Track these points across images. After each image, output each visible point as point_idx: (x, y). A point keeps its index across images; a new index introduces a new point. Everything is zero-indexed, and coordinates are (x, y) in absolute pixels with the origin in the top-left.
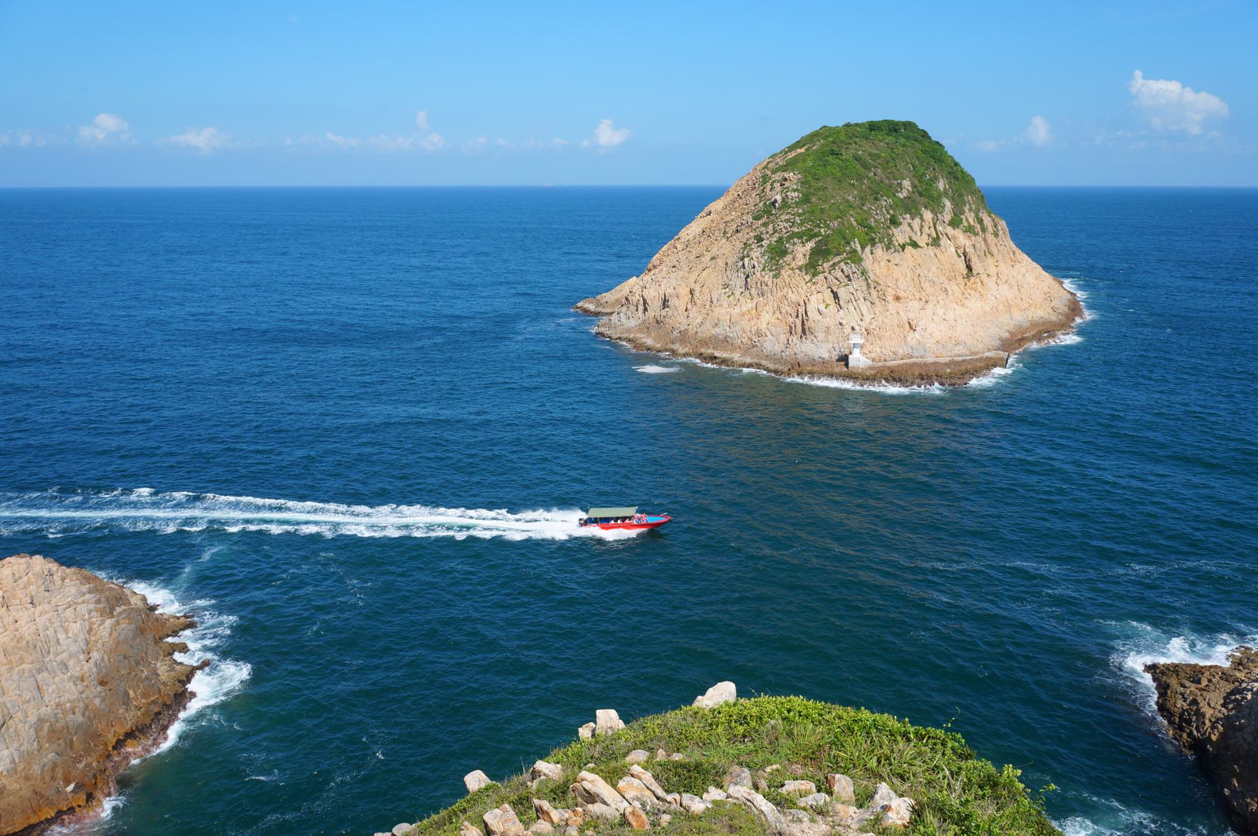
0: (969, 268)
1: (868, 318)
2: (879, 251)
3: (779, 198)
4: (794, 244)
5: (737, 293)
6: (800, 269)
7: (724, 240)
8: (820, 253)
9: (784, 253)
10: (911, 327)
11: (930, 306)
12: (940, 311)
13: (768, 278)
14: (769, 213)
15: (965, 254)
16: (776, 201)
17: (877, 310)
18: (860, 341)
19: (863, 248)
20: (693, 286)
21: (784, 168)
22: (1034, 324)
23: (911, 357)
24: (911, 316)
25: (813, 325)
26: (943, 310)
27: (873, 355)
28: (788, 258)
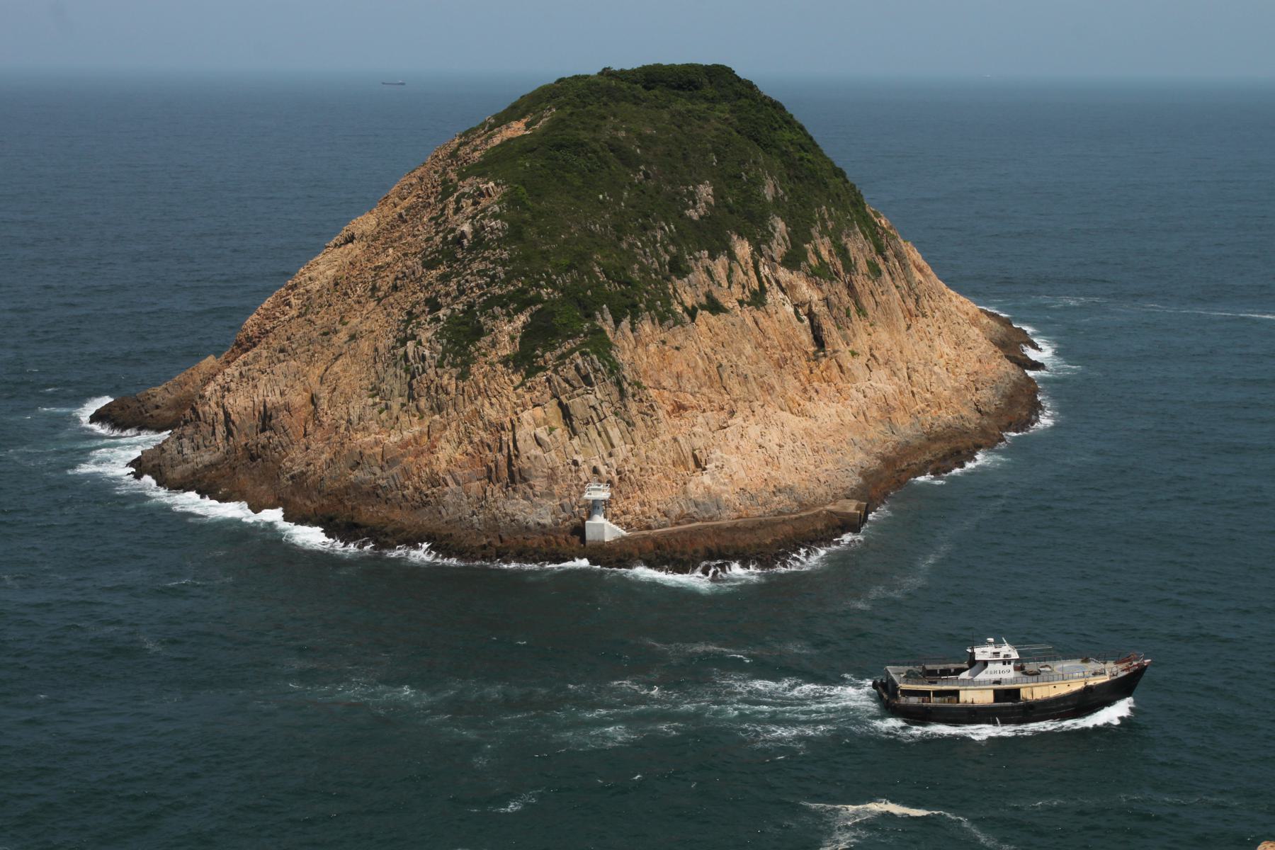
0: (819, 342)
1: (622, 450)
2: (646, 327)
3: (466, 228)
4: (495, 318)
5: (395, 407)
6: (505, 361)
7: (373, 304)
8: (540, 334)
9: (479, 332)
10: (698, 464)
11: (738, 420)
12: (754, 431)
13: (448, 379)
14: (452, 258)
15: (811, 315)
16: (463, 235)
17: (638, 436)
18: (603, 494)
19: (617, 322)
20: (316, 387)
21: (481, 170)
22: (933, 438)
23: (692, 519)
24: (699, 443)
25: (527, 465)
26: (758, 429)
27: (629, 518)
28: (485, 341)
